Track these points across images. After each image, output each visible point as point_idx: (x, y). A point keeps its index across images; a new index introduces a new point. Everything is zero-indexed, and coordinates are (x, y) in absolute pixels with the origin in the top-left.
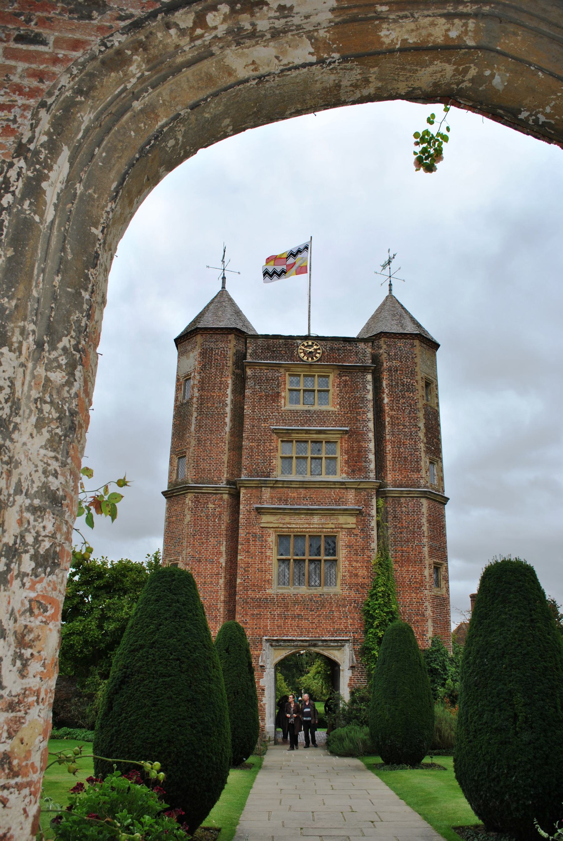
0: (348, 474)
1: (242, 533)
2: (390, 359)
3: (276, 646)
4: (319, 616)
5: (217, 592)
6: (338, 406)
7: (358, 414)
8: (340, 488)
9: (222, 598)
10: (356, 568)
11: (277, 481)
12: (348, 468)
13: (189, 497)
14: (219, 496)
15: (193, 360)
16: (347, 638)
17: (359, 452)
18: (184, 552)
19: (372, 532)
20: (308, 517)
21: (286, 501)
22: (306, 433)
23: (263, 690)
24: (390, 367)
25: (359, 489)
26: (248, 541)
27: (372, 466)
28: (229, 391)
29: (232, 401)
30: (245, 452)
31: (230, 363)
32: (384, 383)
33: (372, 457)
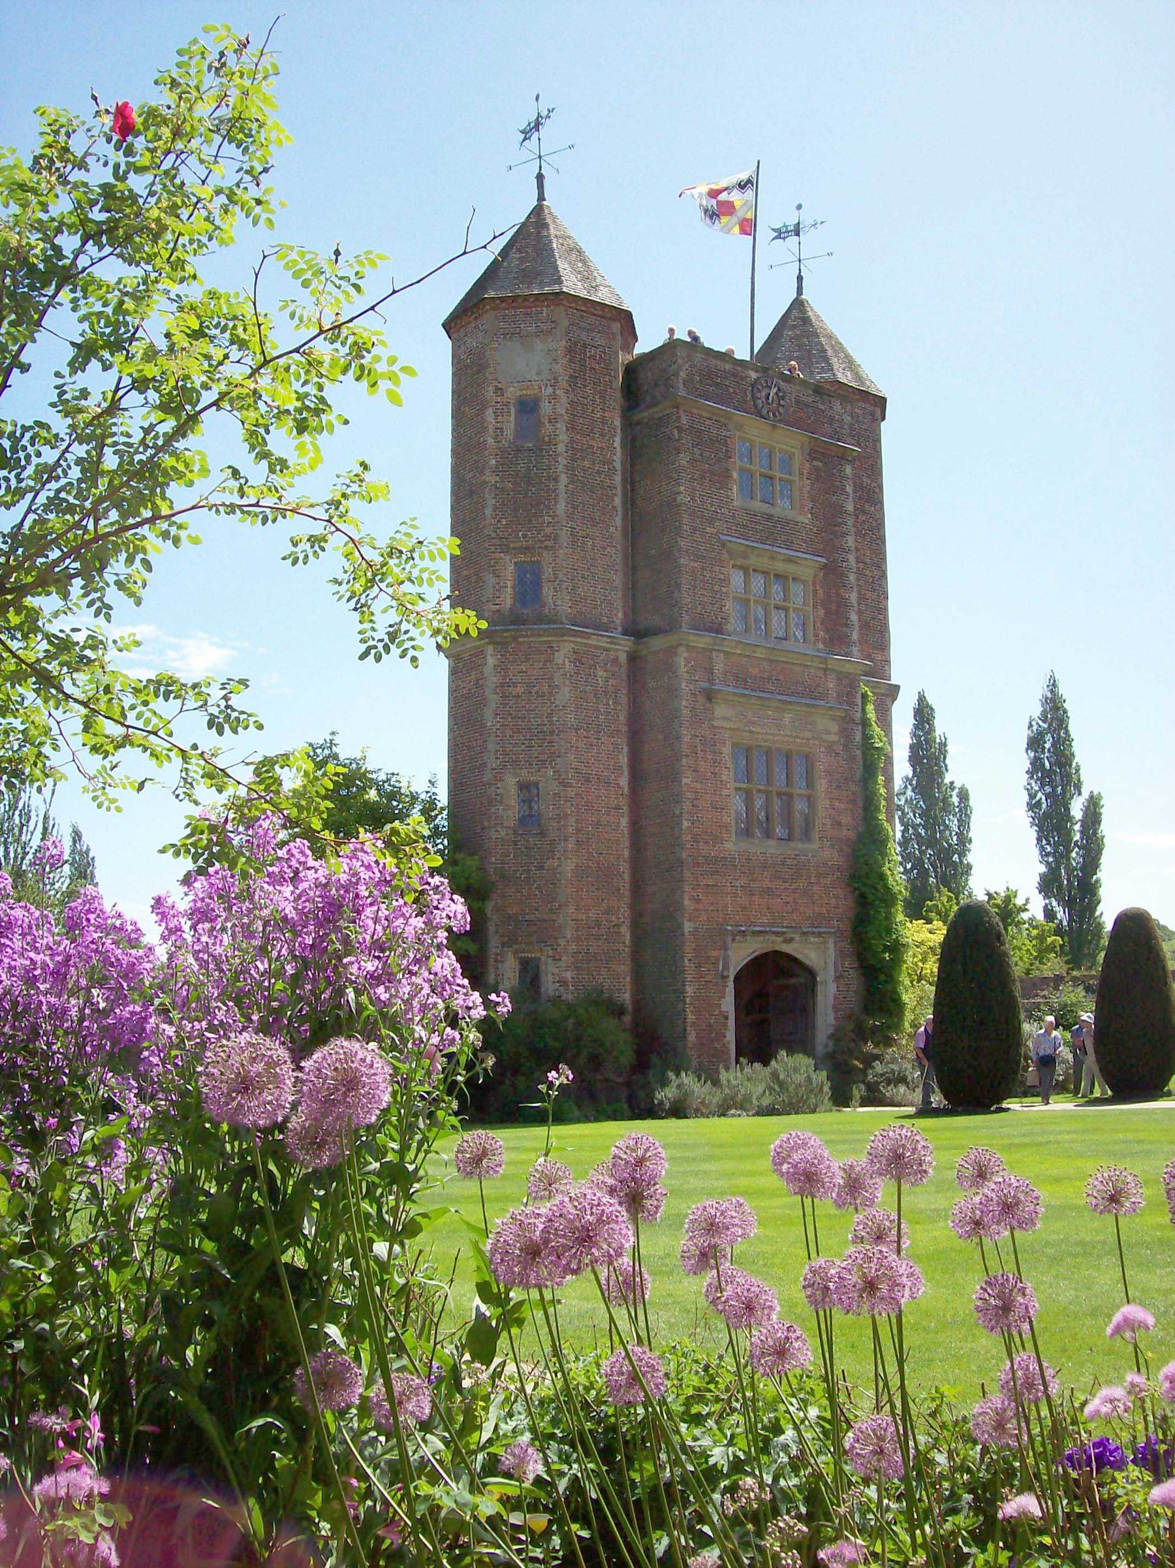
0: (824, 643)
23: (727, 1018)
28: (618, 440)
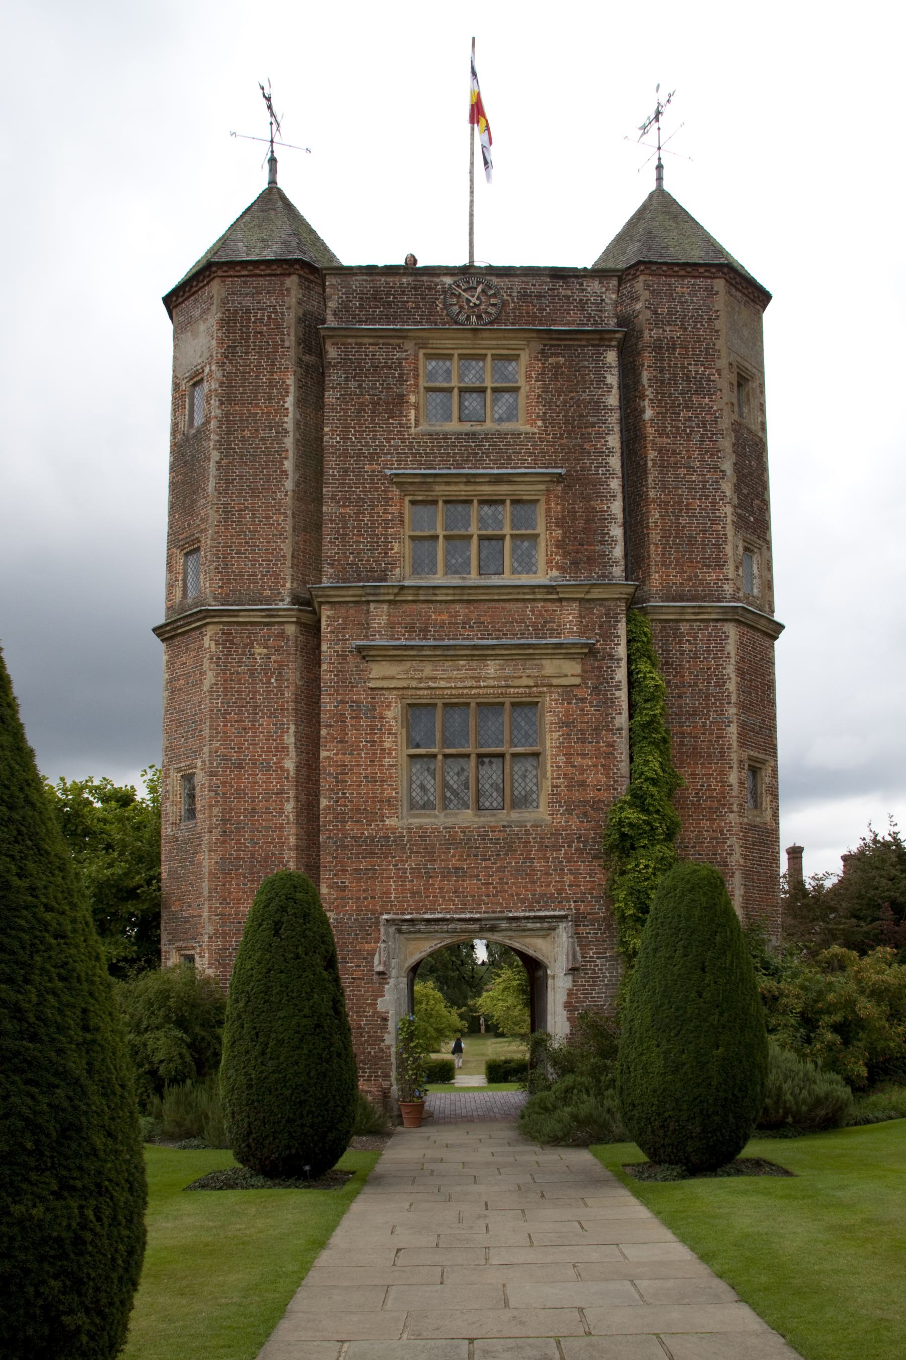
0: (562, 568)
1: (328, 703)
2: (658, 321)
3: (410, 932)
4: (501, 869)
5: (281, 828)
6: (540, 423)
7: (586, 438)
8: (545, 600)
9: (292, 840)
10: (582, 770)
11: (402, 588)
12: (564, 556)
13: (209, 634)
14: (276, 629)
15: (206, 338)
16: (562, 913)
17: (587, 521)
18: (206, 749)
19: (617, 693)
20: (475, 664)
21: (425, 630)
22: (467, 483)
23: (385, 1019)
24: (659, 339)
25: (589, 600)
26: (342, 718)
27: (618, 552)
29: (297, 424)
30: (328, 530)
31: (290, 341)
32: (645, 375)
33: (617, 532)
